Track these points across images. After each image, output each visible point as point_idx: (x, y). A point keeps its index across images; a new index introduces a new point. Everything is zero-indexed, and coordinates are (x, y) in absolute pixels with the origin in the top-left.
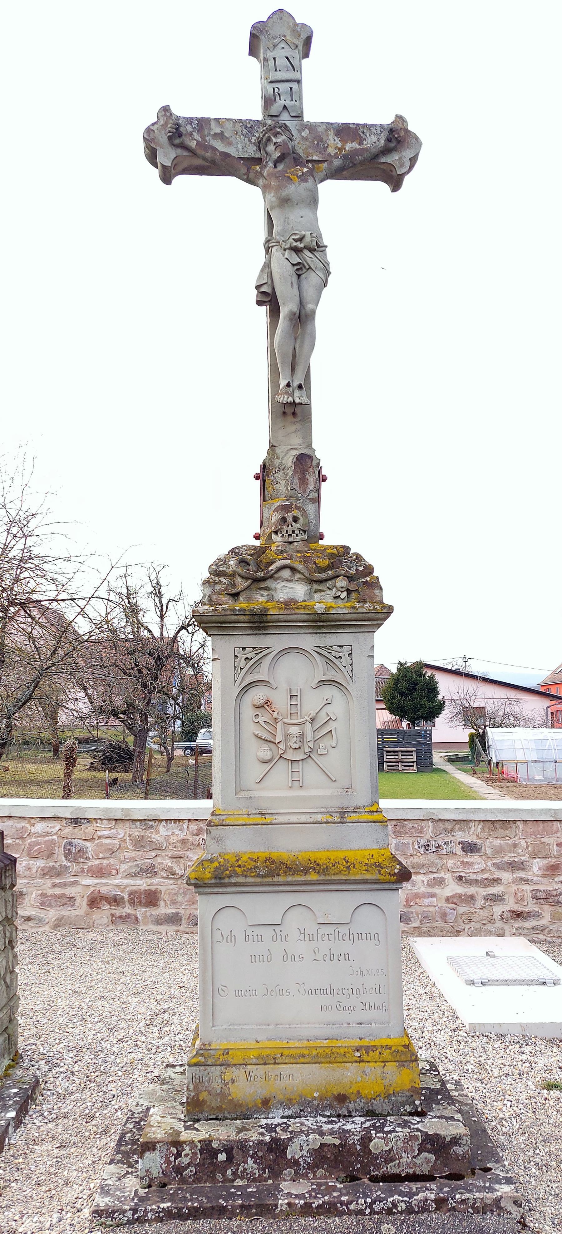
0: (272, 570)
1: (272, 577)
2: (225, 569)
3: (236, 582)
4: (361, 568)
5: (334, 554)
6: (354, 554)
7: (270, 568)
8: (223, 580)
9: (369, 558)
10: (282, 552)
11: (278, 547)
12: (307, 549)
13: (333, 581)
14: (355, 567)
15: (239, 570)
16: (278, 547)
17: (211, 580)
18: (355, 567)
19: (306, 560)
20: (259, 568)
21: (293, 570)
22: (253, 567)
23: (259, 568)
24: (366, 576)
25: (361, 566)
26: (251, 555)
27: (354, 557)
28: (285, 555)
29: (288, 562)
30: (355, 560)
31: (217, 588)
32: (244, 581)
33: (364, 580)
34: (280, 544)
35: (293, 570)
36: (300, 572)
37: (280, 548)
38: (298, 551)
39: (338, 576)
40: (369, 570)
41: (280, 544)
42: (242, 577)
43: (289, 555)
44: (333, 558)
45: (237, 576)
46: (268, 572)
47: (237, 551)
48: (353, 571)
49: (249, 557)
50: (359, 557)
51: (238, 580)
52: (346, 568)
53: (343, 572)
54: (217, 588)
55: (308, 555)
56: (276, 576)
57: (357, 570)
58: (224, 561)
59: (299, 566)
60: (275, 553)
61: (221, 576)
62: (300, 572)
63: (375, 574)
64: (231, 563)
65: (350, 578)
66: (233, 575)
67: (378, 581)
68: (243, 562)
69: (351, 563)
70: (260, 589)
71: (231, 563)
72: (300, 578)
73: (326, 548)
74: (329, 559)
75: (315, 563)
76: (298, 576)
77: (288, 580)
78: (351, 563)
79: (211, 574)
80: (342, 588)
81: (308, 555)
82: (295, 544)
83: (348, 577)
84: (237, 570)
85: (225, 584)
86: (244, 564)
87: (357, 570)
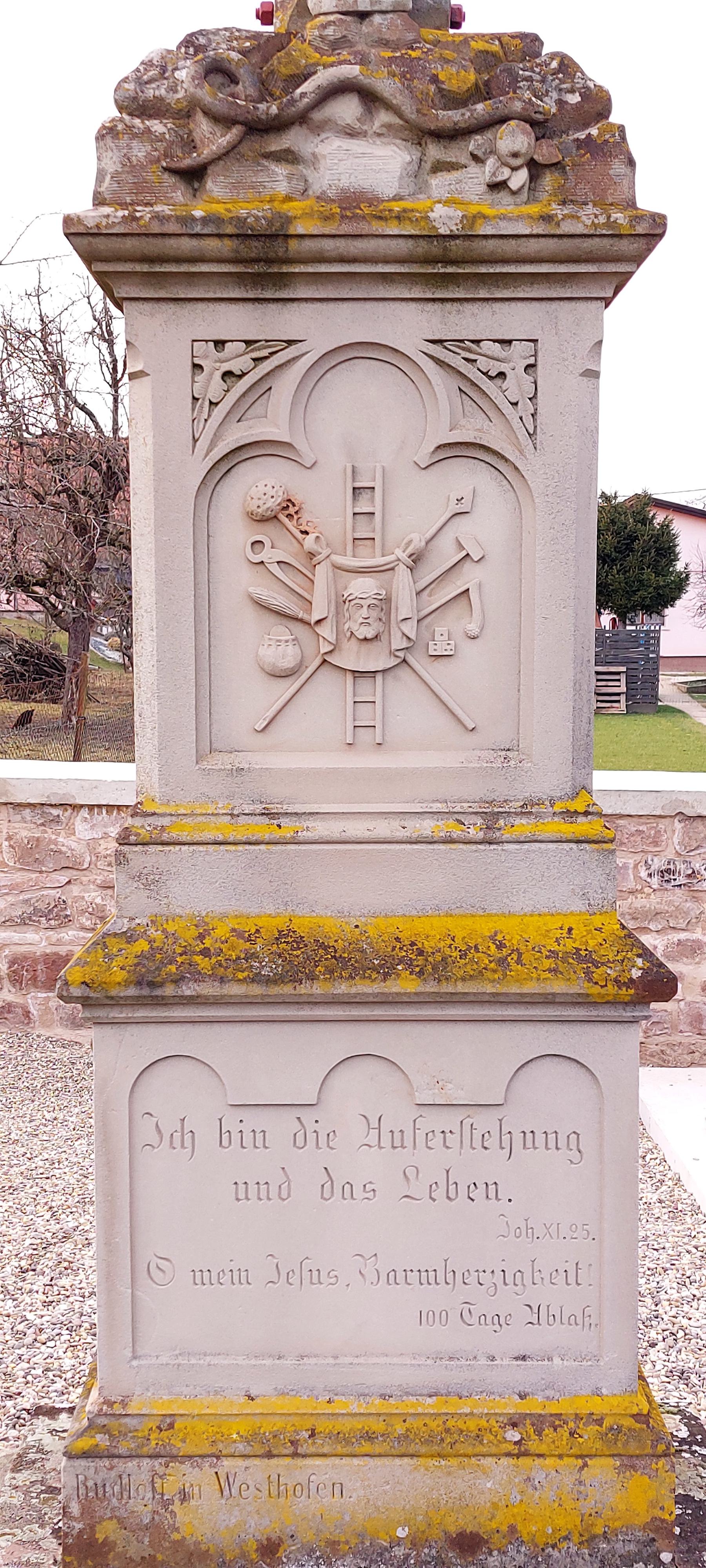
0: (303, 95)
1: (303, 119)
2: (163, 92)
3: (197, 136)
4: (574, 99)
5: (494, 55)
6: (553, 56)
7: (299, 91)
8: (157, 126)
9: (596, 70)
10: (336, 45)
11: (324, 26)
12: (410, 36)
13: (489, 135)
14: (555, 95)
15: (205, 94)
16: (324, 26)
17: (120, 127)
18: (555, 95)
19: (408, 71)
20: (265, 93)
21: (370, 98)
22: (246, 87)
23: (265, 93)
24: (586, 125)
25: (572, 91)
26: (244, 53)
27: (554, 64)
28: (345, 54)
29: (352, 71)
30: (555, 73)
31: (140, 151)
32: (218, 131)
33: (582, 135)
34: (332, 18)
35: (370, 98)
36: (389, 106)
37: (330, 31)
38: (384, 43)
39: (503, 120)
40: (597, 104)
41: (332, 18)
42: (216, 118)
43: (355, 54)
44: (489, 67)
45: (200, 117)
46: (293, 102)
47: (202, 41)
48: (549, 105)
49: (234, 55)
50: (566, 66)
51: (203, 126)
52: (527, 95)
53: (518, 106)
54: (140, 151)
55: (414, 54)
56: (317, 116)
57: (560, 103)
58: (161, 68)
59: (386, 85)
60: (317, 49)
61: (150, 117)
62: (389, 106)
63: (615, 118)
64: (181, 75)
65: (540, 127)
66: (184, 114)
67: (623, 138)
68: (217, 71)
69: (543, 81)
70: (268, 156)
71: (181, 75)
72: (389, 126)
73: (467, 39)
74: (478, 71)
75: (435, 79)
76: (384, 117)
77: (351, 133)
78: (543, 81)
79: (121, 109)
80: (515, 155)
81: (414, 54)
82: (377, 19)
83: (533, 123)
84: (199, 93)
85: (161, 138)
86: (219, 79)
87: (560, 103)
